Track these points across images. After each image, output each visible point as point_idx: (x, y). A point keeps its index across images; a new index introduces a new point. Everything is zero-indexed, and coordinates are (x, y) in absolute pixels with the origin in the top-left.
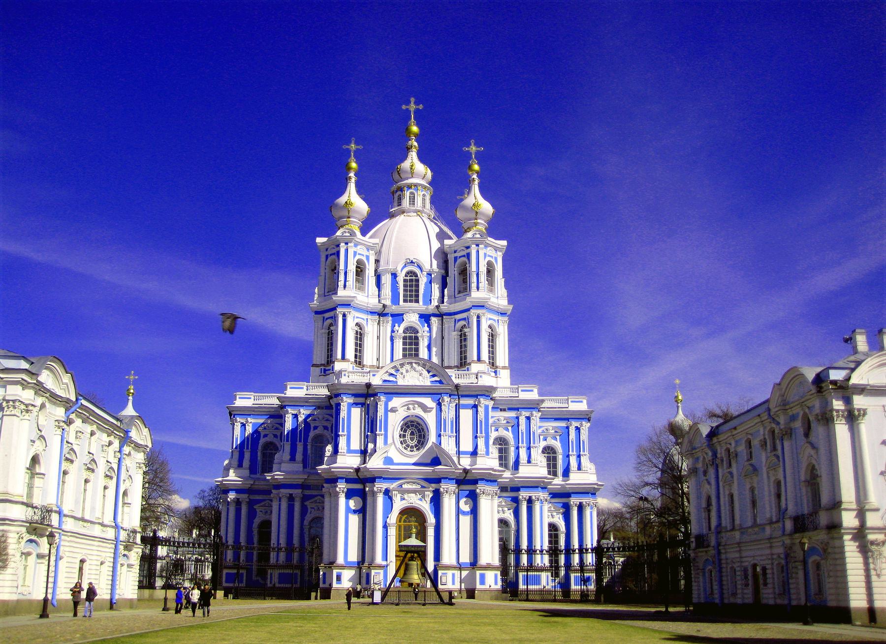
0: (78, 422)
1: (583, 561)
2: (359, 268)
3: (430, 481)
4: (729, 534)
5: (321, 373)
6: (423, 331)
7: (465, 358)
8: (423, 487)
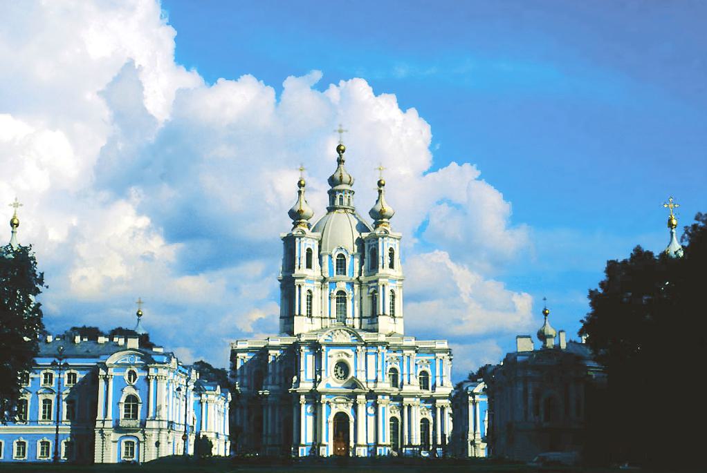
6: (349, 296)
7: (376, 313)
8: (347, 400)
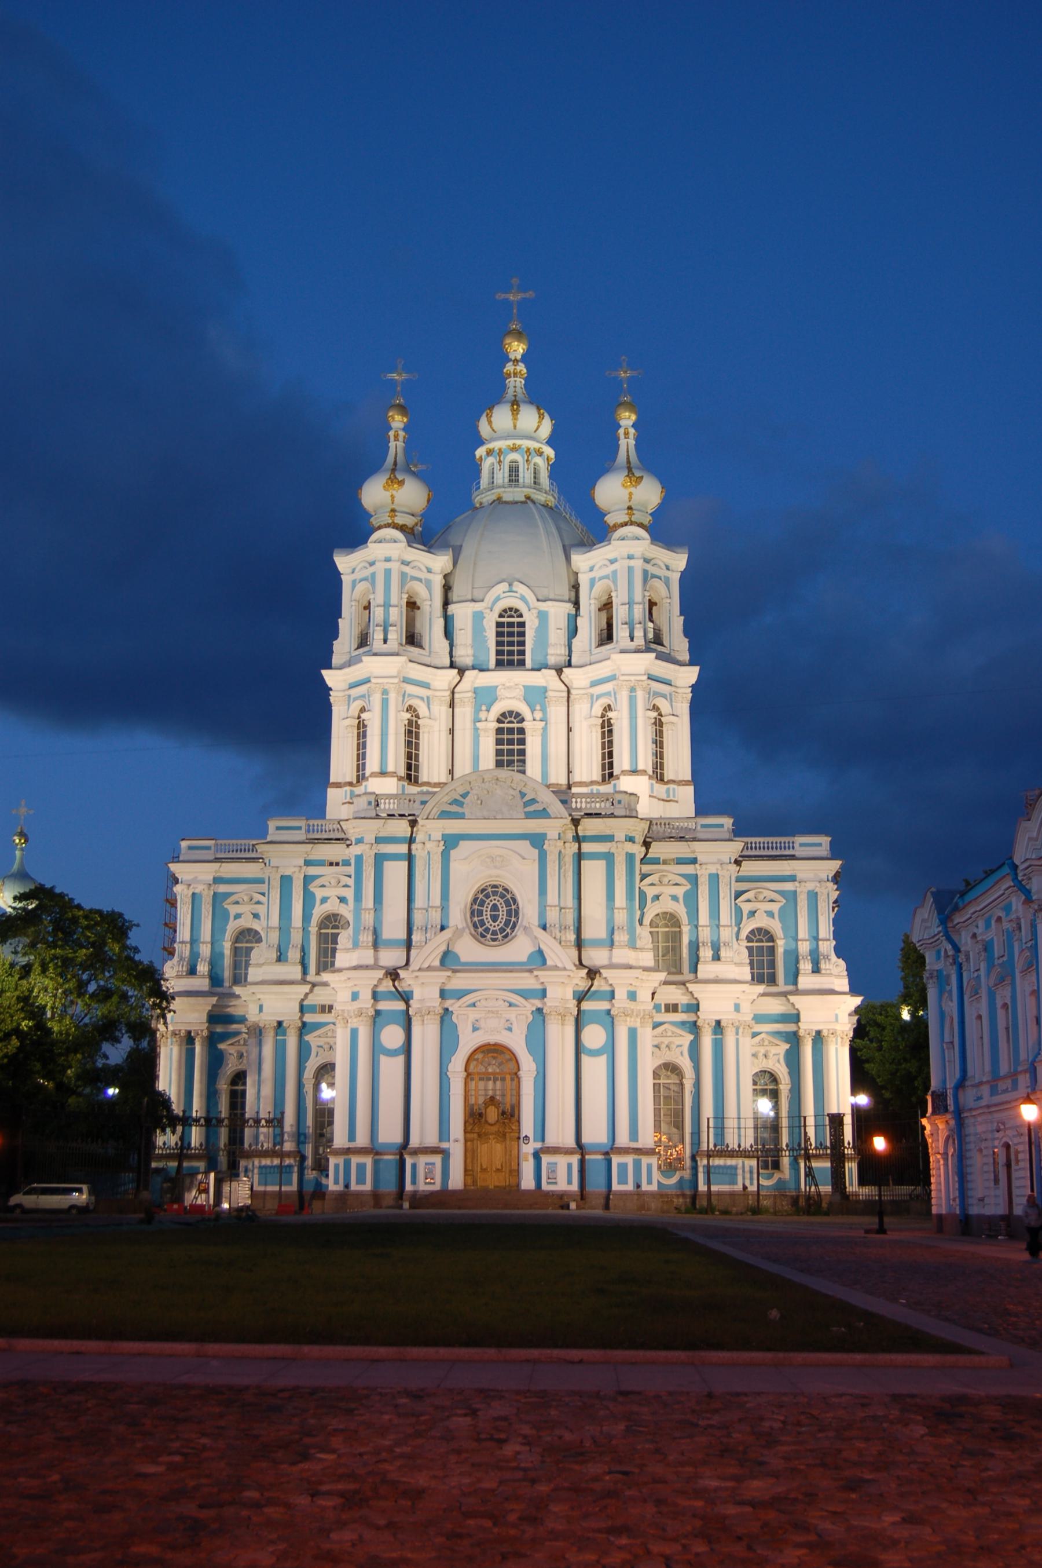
1: (809, 1139)
2: (414, 603)
3: (525, 994)
5: (346, 799)
7: (611, 765)
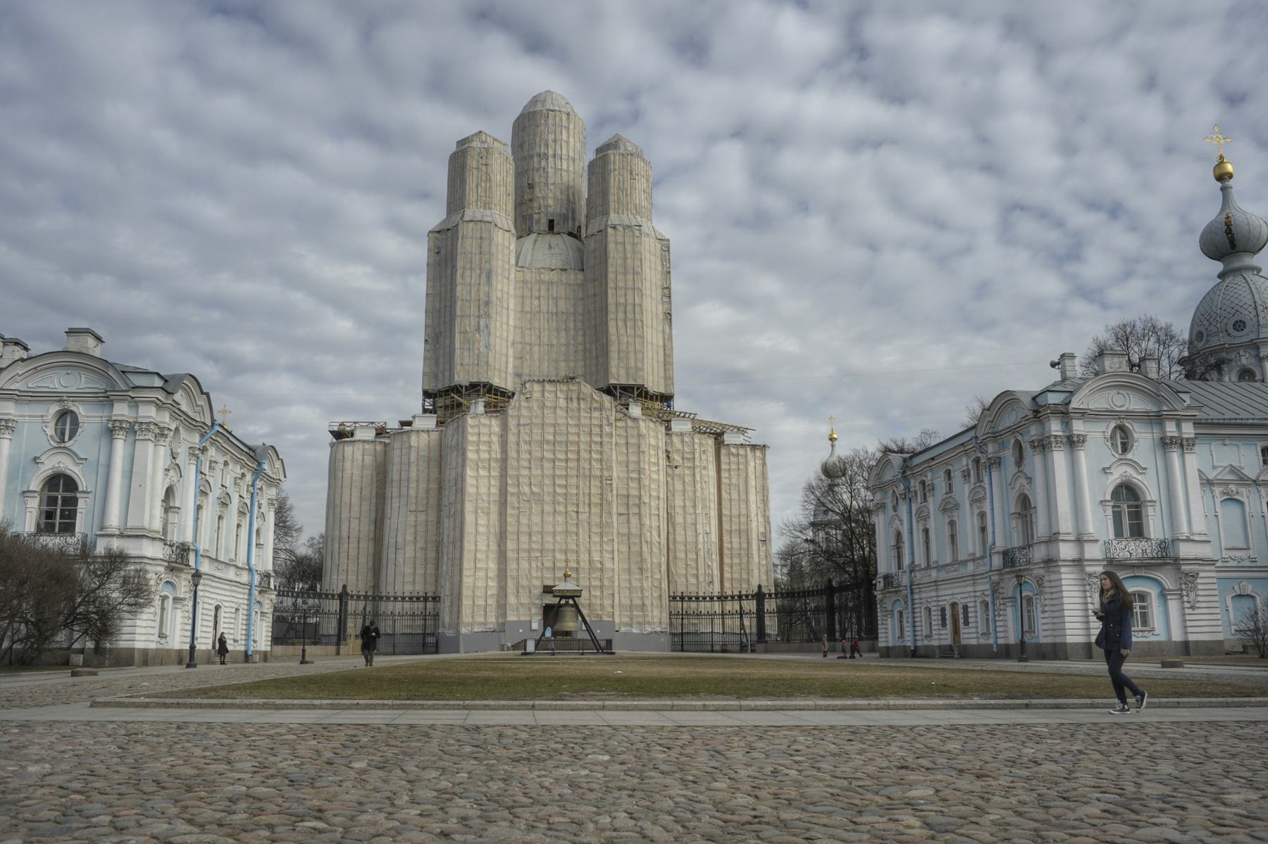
0: (212, 452)
4: (922, 572)
